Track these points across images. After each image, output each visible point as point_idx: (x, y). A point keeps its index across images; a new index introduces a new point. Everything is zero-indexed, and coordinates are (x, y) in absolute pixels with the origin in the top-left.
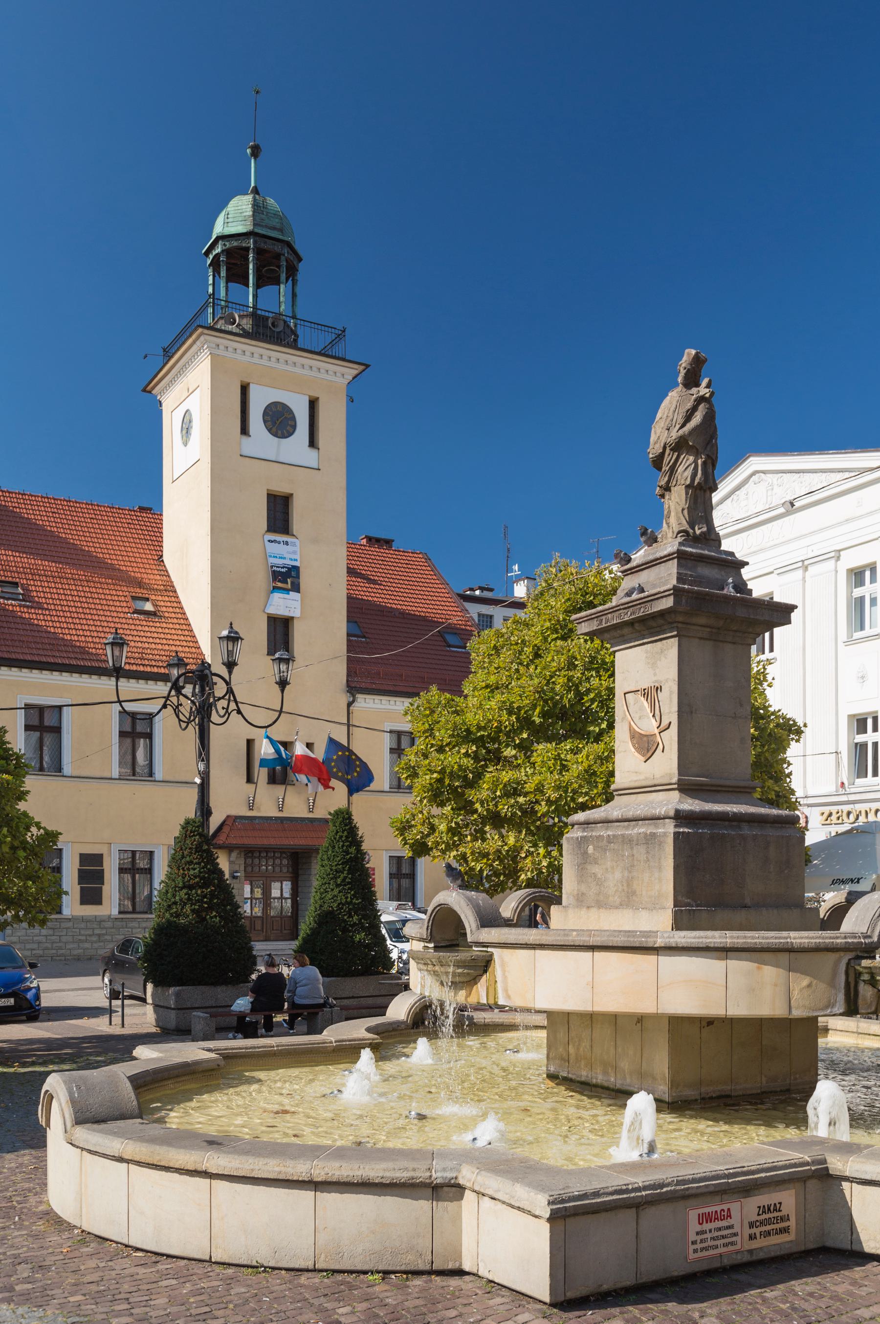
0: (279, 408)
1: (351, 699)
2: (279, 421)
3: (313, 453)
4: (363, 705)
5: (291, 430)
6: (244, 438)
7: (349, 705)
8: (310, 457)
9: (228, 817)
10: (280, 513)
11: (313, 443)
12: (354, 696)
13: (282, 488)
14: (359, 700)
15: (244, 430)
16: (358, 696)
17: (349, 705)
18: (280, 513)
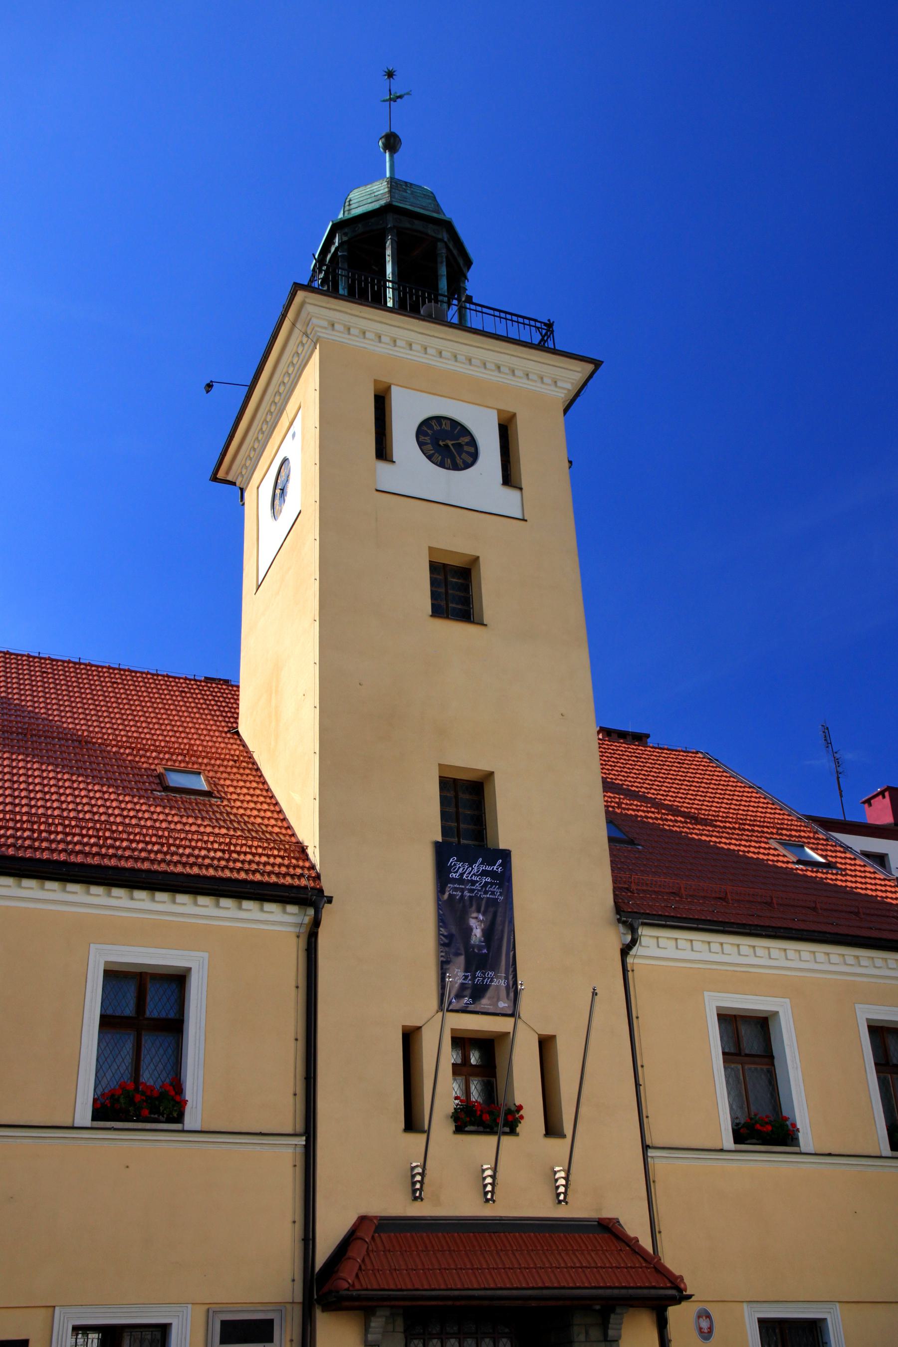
0: (446, 426)
1: (629, 938)
2: (447, 443)
3: (512, 495)
4: (653, 951)
5: (469, 460)
6: (382, 466)
7: (625, 951)
8: (507, 501)
9: (363, 1220)
10: (455, 590)
11: (509, 478)
12: (633, 930)
13: (457, 544)
14: (644, 941)
15: (383, 452)
16: (644, 931)
17: (625, 951)
18: (455, 590)
